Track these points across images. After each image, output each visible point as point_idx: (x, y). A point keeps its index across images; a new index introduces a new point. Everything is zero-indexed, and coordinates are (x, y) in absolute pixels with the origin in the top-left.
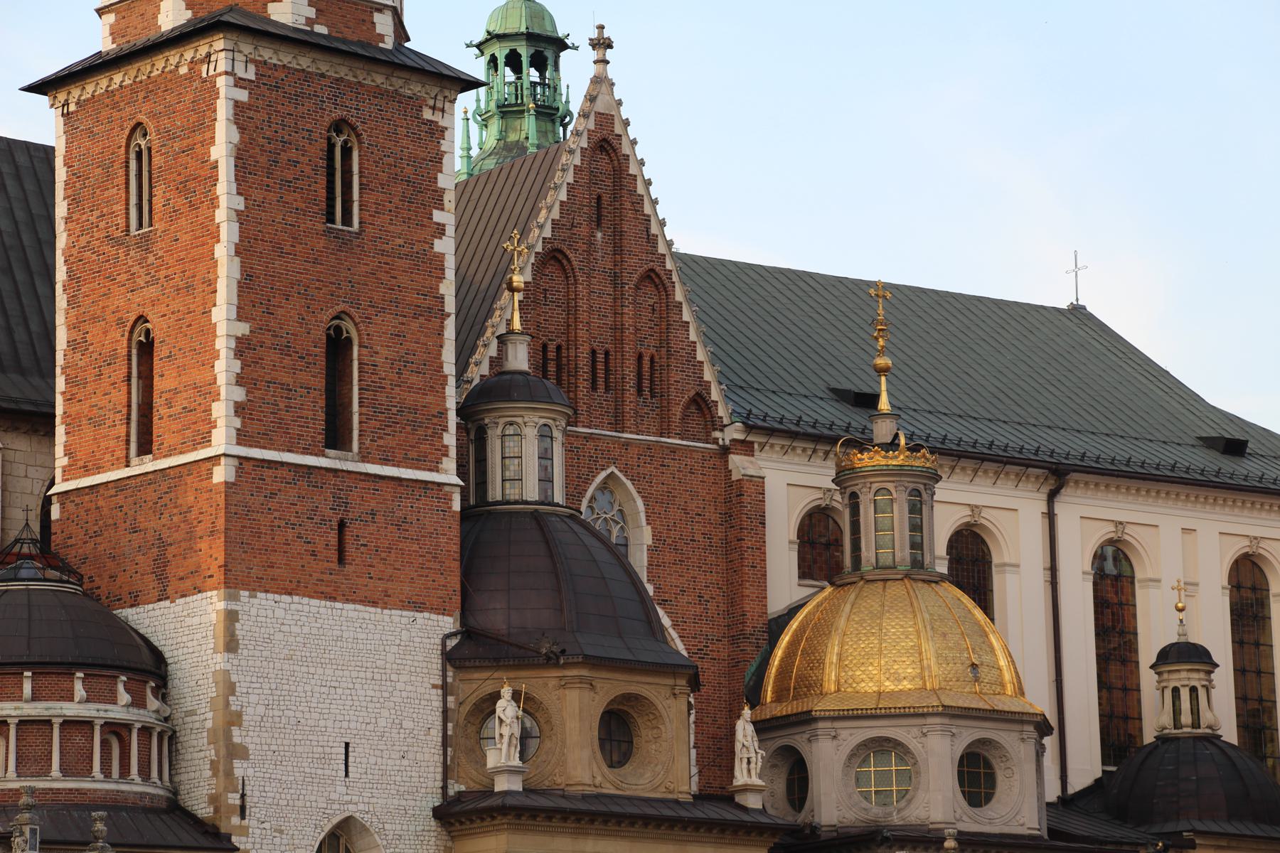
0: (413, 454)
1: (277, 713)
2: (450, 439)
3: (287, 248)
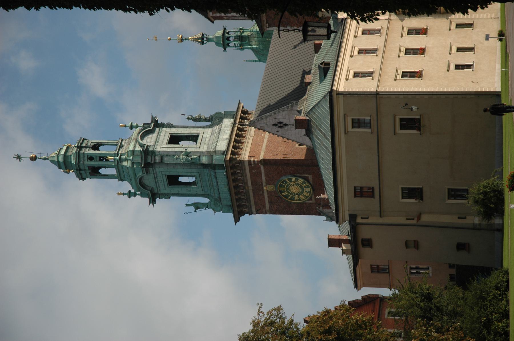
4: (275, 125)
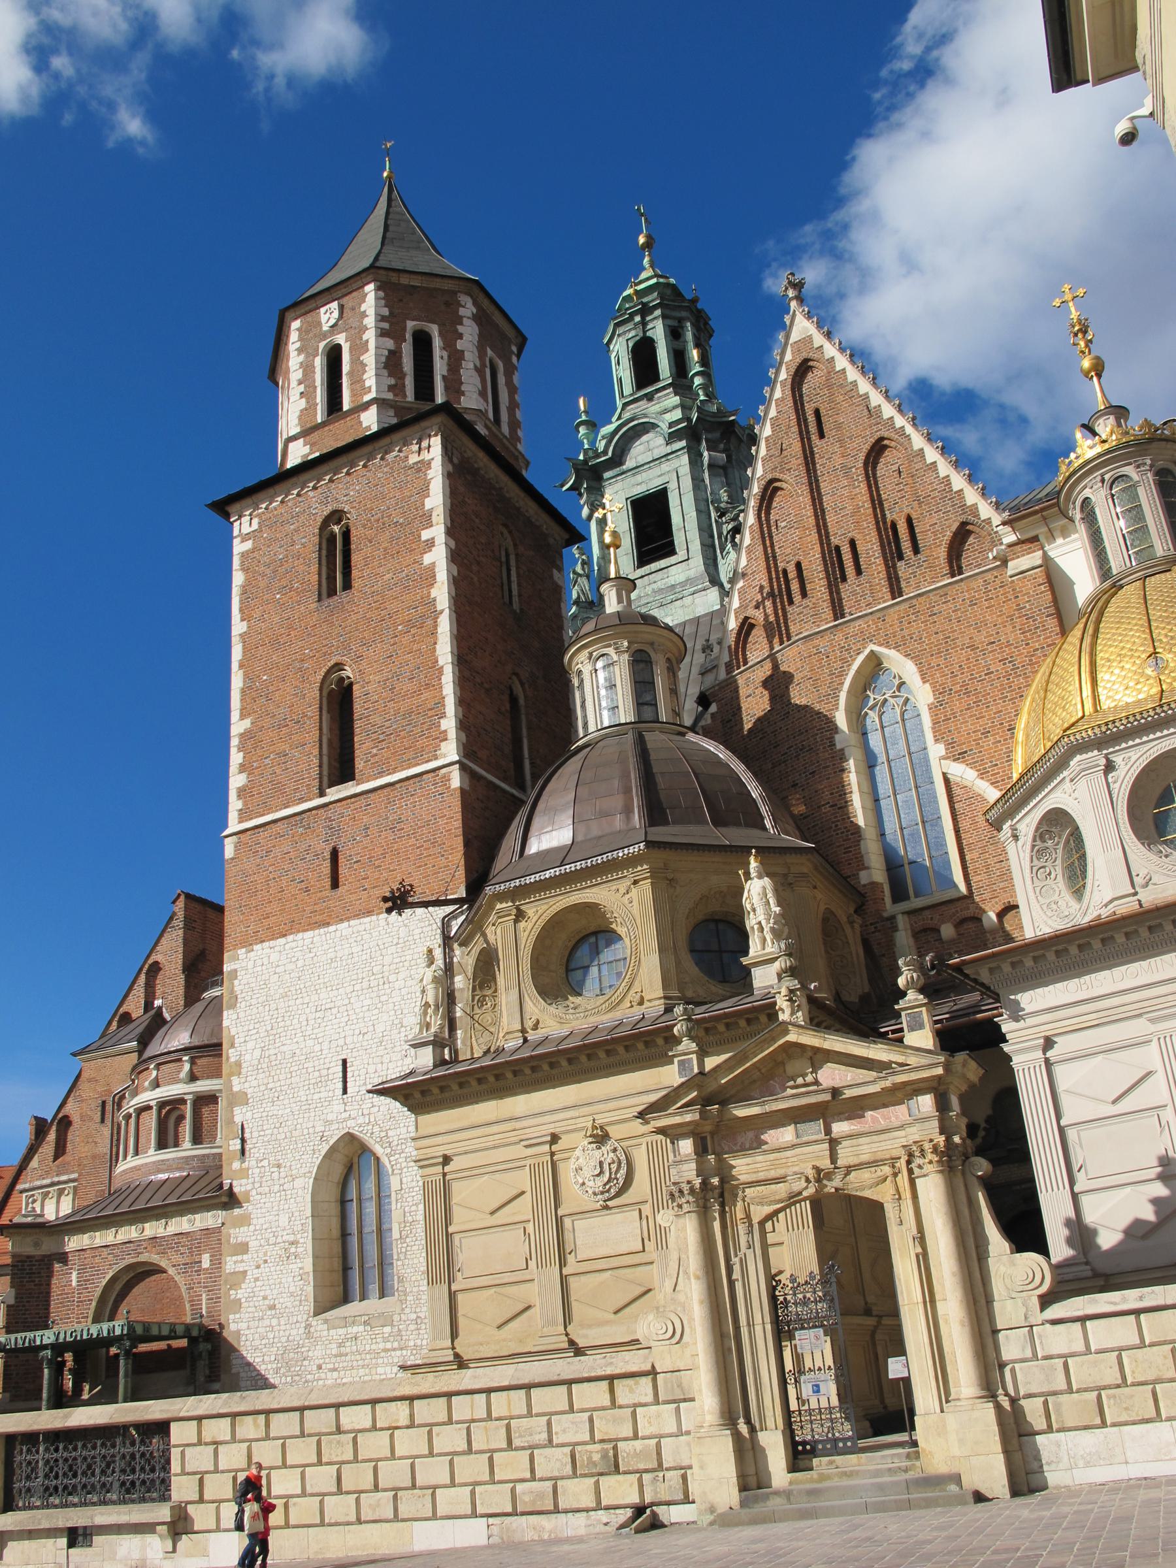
0: (411, 754)
1: (272, 1052)
2: (449, 724)
3: (286, 639)
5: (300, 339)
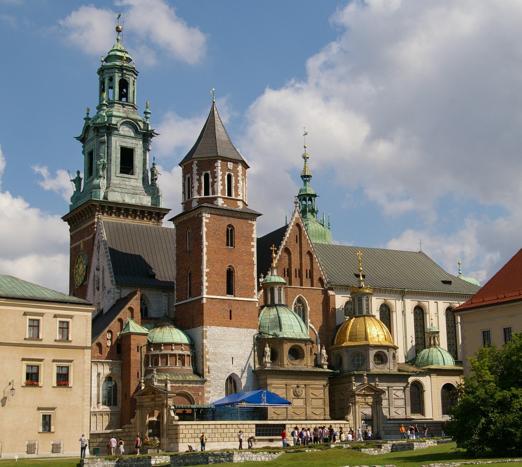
2: (256, 291)
3: (217, 252)
4: (99, 242)
5: (221, 166)
